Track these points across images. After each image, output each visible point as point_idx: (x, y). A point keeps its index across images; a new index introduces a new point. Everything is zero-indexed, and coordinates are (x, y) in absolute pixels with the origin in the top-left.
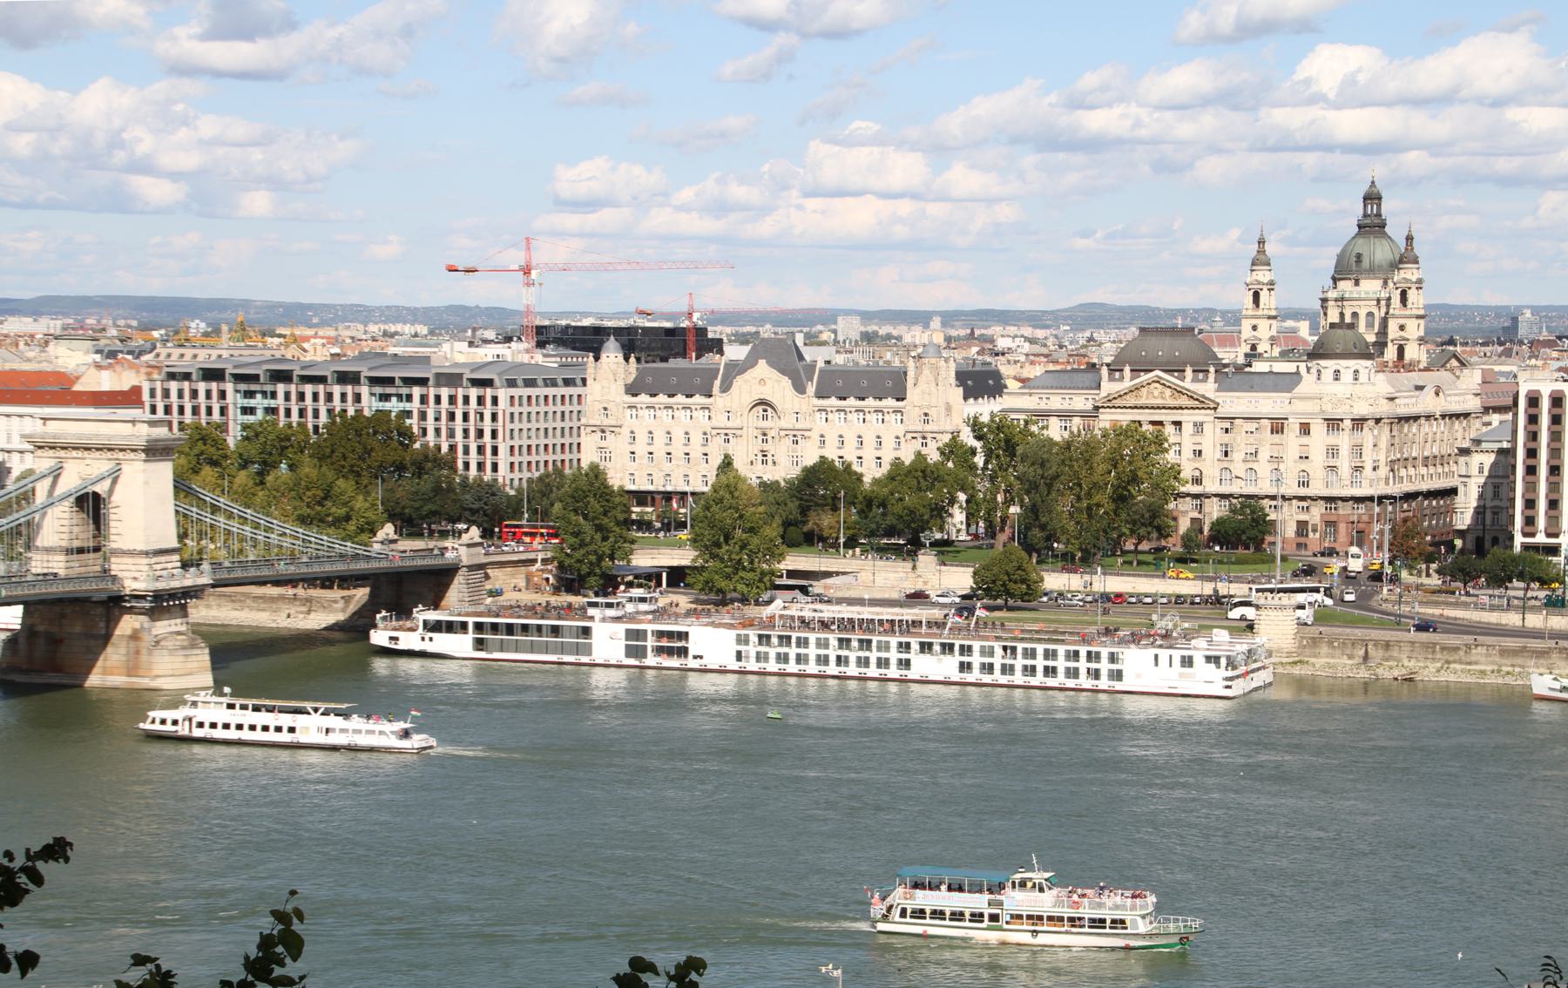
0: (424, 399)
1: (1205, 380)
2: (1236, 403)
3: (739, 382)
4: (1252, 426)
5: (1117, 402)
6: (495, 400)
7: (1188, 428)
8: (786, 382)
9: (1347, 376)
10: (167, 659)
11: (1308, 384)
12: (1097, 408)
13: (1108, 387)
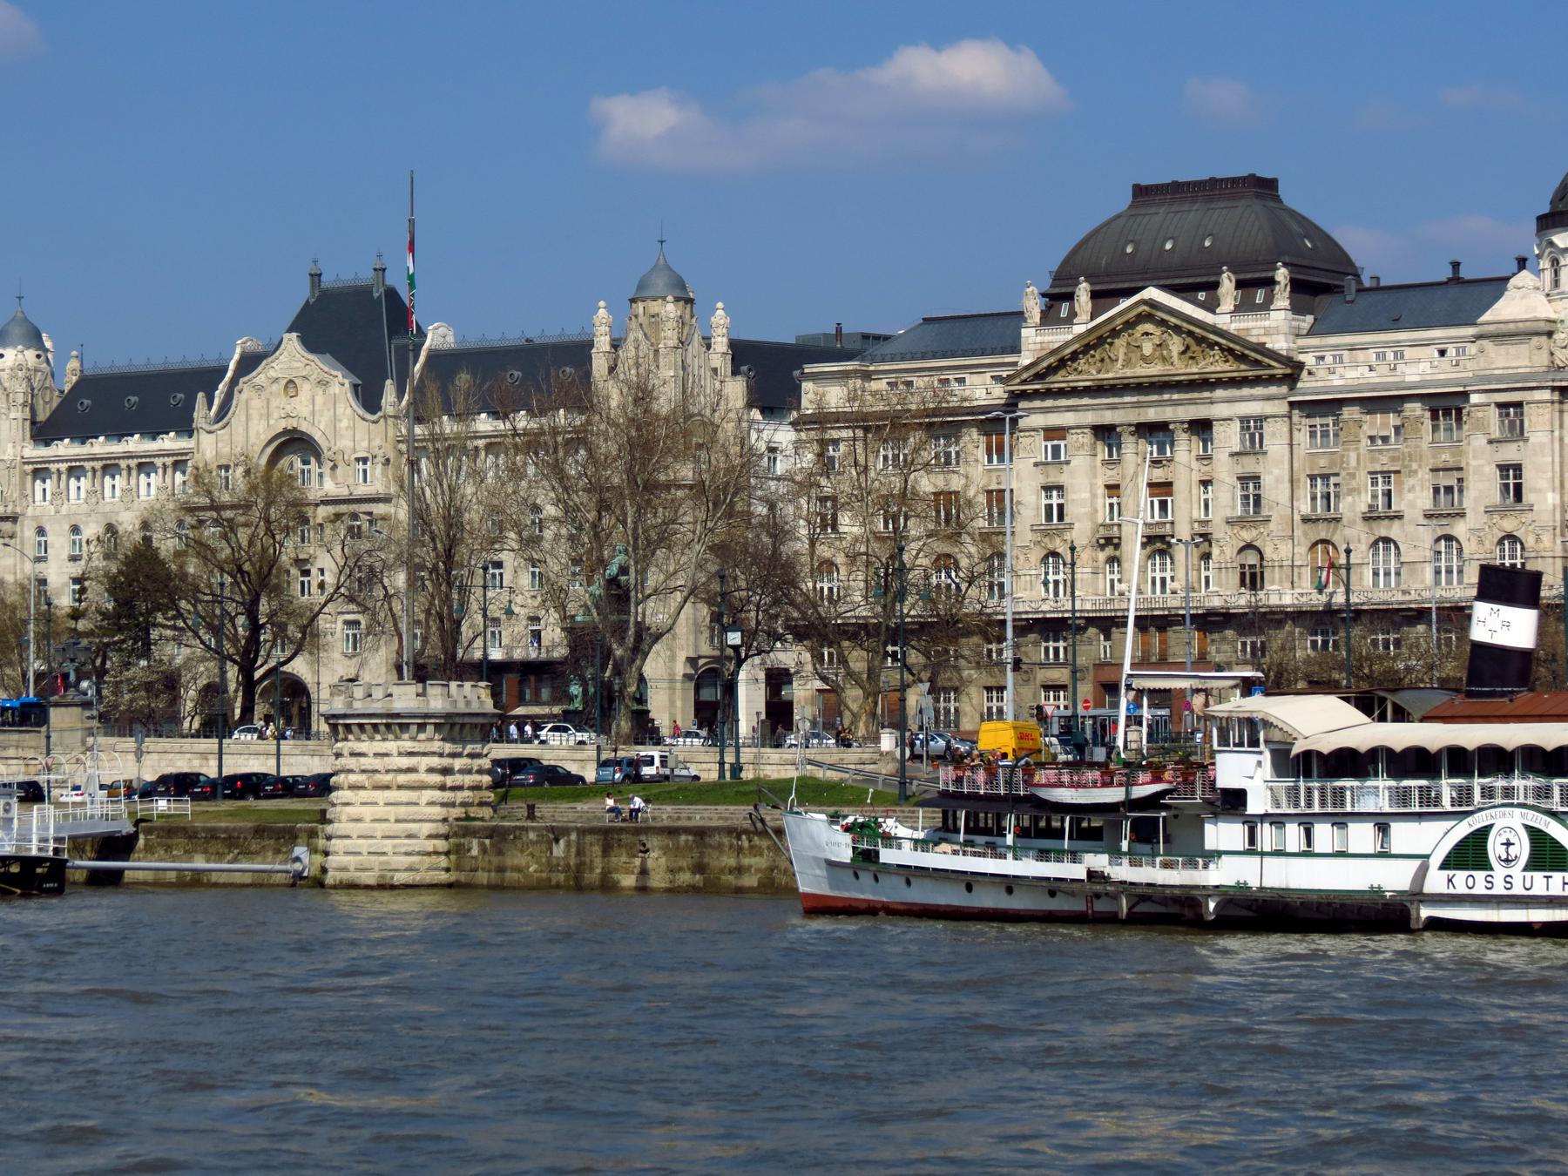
1: (1266, 306)
2: (1347, 364)
4: (1383, 423)
5: (1059, 380)
7: (1228, 437)
8: (340, 384)
11: (1522, 301)
12: (1015, 398)
13: (1036, 341)
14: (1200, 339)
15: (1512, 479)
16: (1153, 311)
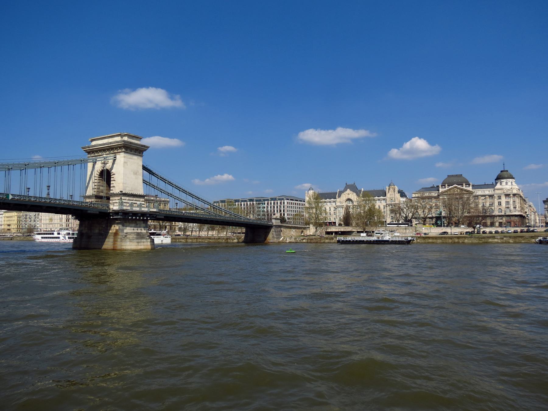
0: (268, 204)
3: (343, 195)
4: (484, 198)
6: (284, 203)
8: (355, 194)
9: (509, 184)
10: (128, 243)
12: (439, 195)
14: (462, 190)
15: (500, 204)
16: (456, 187)
